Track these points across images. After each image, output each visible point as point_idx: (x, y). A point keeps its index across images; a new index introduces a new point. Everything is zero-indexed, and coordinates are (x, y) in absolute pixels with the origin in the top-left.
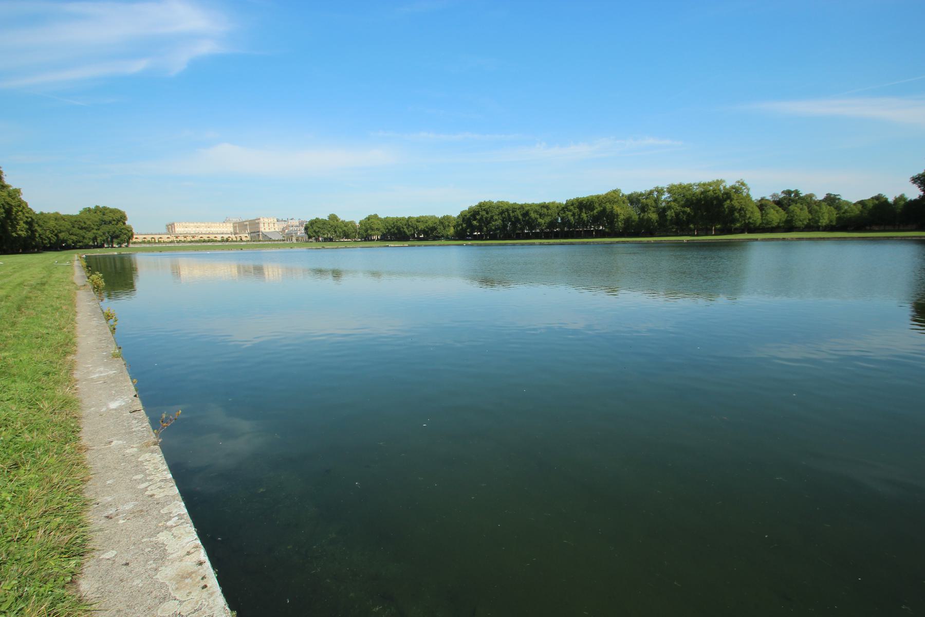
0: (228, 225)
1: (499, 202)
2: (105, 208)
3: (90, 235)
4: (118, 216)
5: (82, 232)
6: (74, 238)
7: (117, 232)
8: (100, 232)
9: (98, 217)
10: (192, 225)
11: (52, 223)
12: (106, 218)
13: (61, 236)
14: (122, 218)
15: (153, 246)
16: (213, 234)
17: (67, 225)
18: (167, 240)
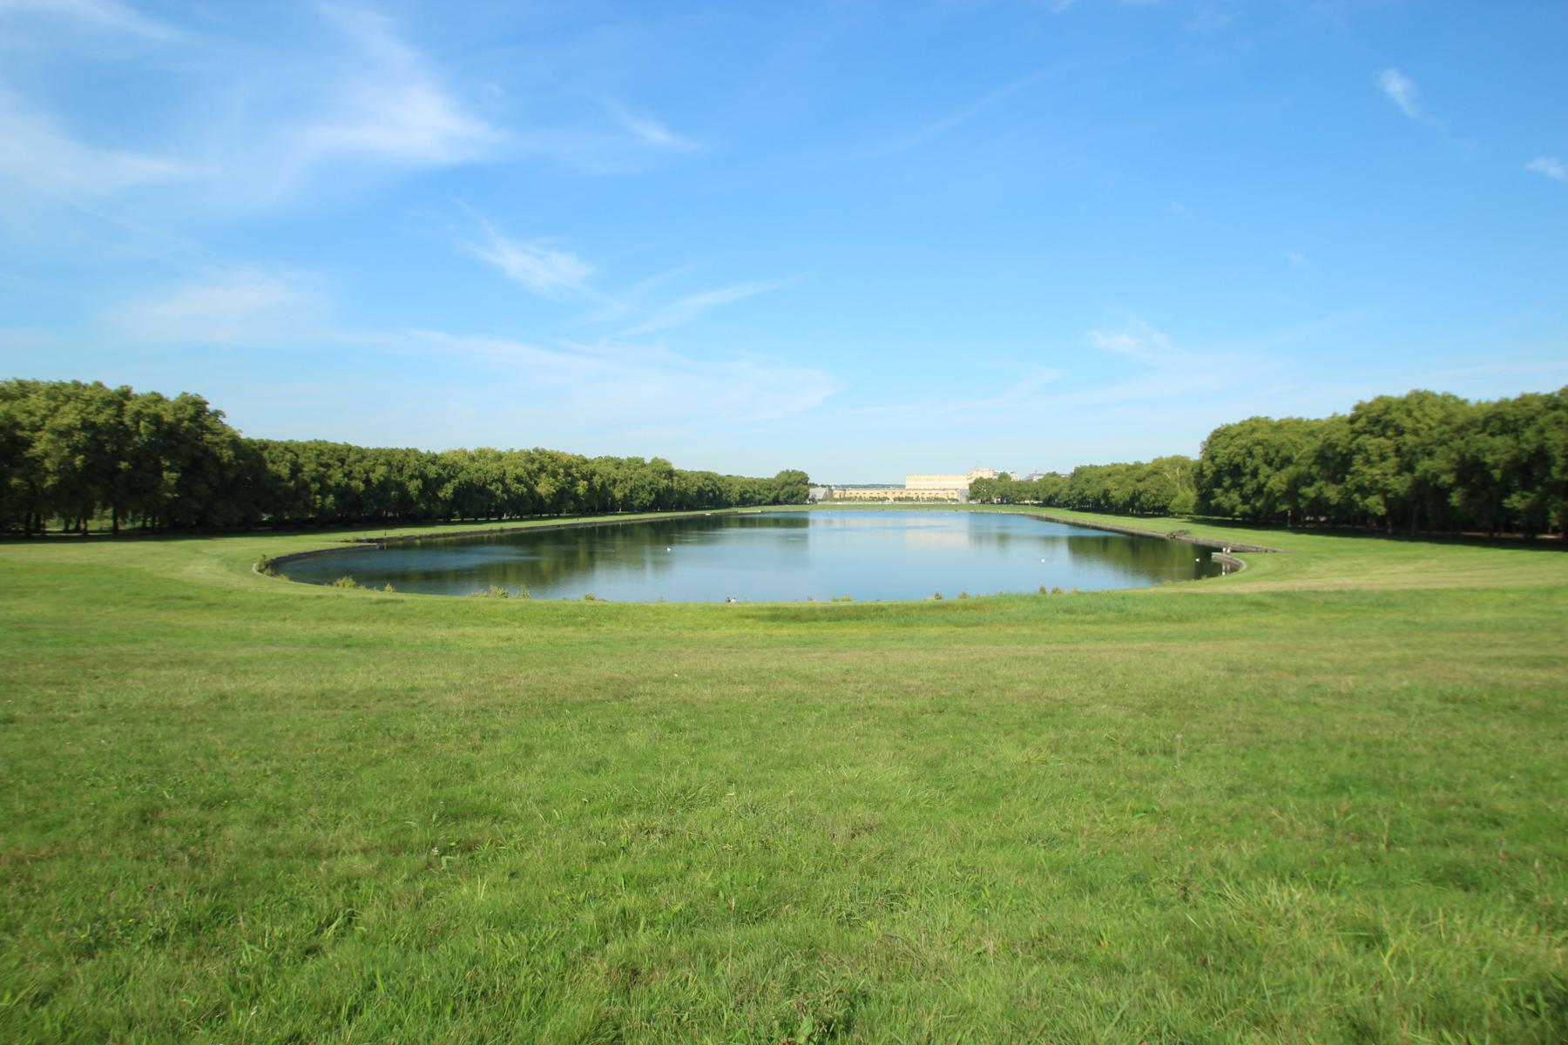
0: (962, 477)
1: (1155, 461)
2: (793, 471)
3: (772, 495)
4: (799, 479)
5: (766, 493)
6: (759, 497)
7: (795, 492)
8: (782, 492)
9: (785, 477)
10: (923, 477)
11: (738, 487)
12: (790, 481)
13: (747, 496)
14: (803, 480)
15: (845, 501)
16: (934, 489)
17: (756, 487)
18: (867, 496)
